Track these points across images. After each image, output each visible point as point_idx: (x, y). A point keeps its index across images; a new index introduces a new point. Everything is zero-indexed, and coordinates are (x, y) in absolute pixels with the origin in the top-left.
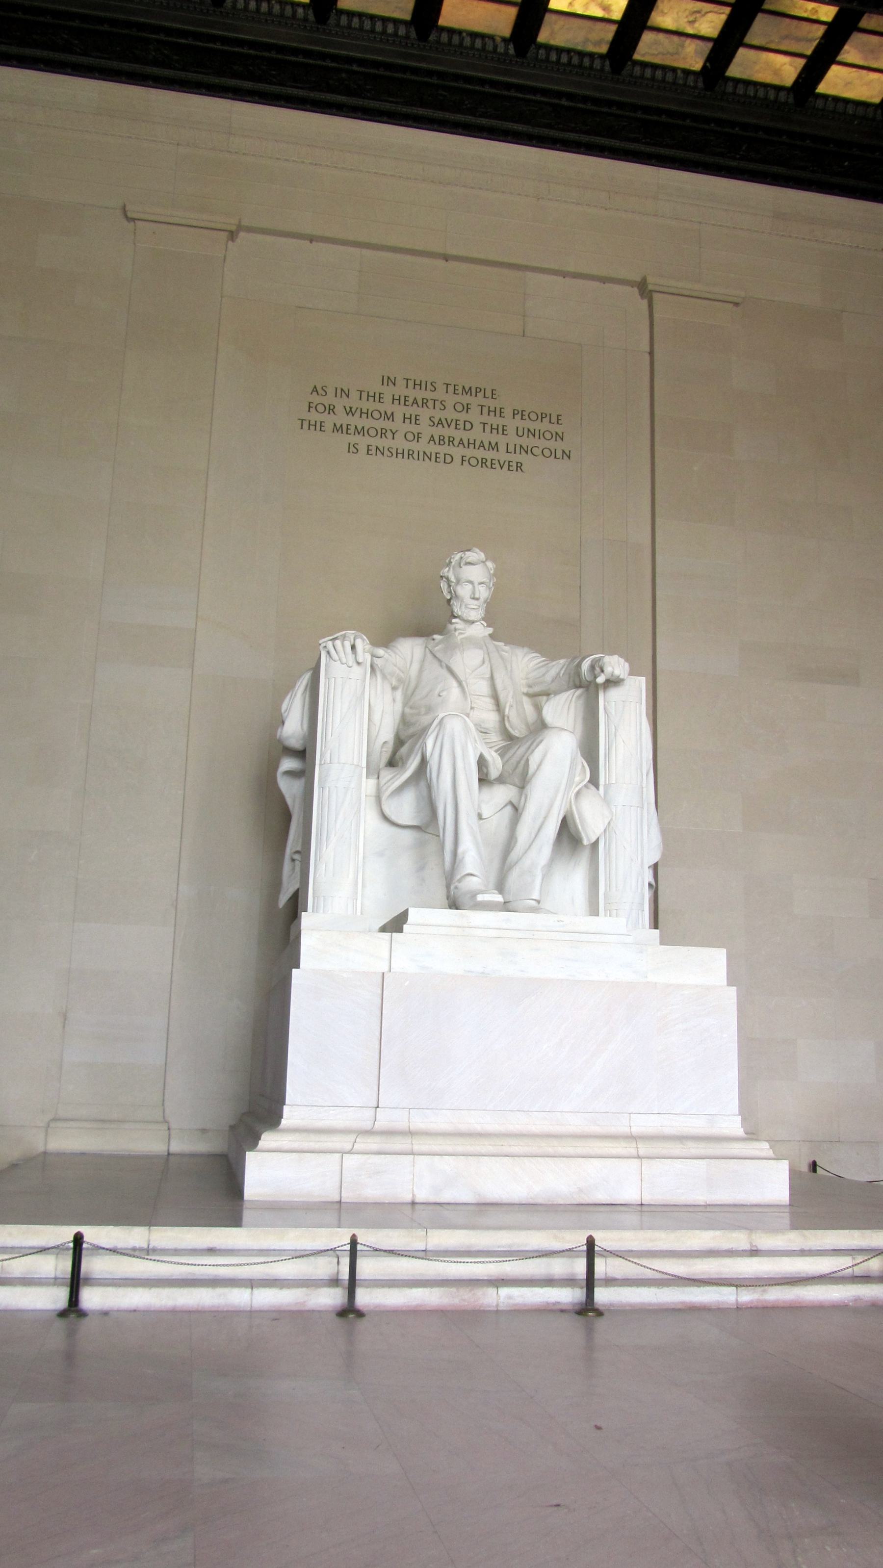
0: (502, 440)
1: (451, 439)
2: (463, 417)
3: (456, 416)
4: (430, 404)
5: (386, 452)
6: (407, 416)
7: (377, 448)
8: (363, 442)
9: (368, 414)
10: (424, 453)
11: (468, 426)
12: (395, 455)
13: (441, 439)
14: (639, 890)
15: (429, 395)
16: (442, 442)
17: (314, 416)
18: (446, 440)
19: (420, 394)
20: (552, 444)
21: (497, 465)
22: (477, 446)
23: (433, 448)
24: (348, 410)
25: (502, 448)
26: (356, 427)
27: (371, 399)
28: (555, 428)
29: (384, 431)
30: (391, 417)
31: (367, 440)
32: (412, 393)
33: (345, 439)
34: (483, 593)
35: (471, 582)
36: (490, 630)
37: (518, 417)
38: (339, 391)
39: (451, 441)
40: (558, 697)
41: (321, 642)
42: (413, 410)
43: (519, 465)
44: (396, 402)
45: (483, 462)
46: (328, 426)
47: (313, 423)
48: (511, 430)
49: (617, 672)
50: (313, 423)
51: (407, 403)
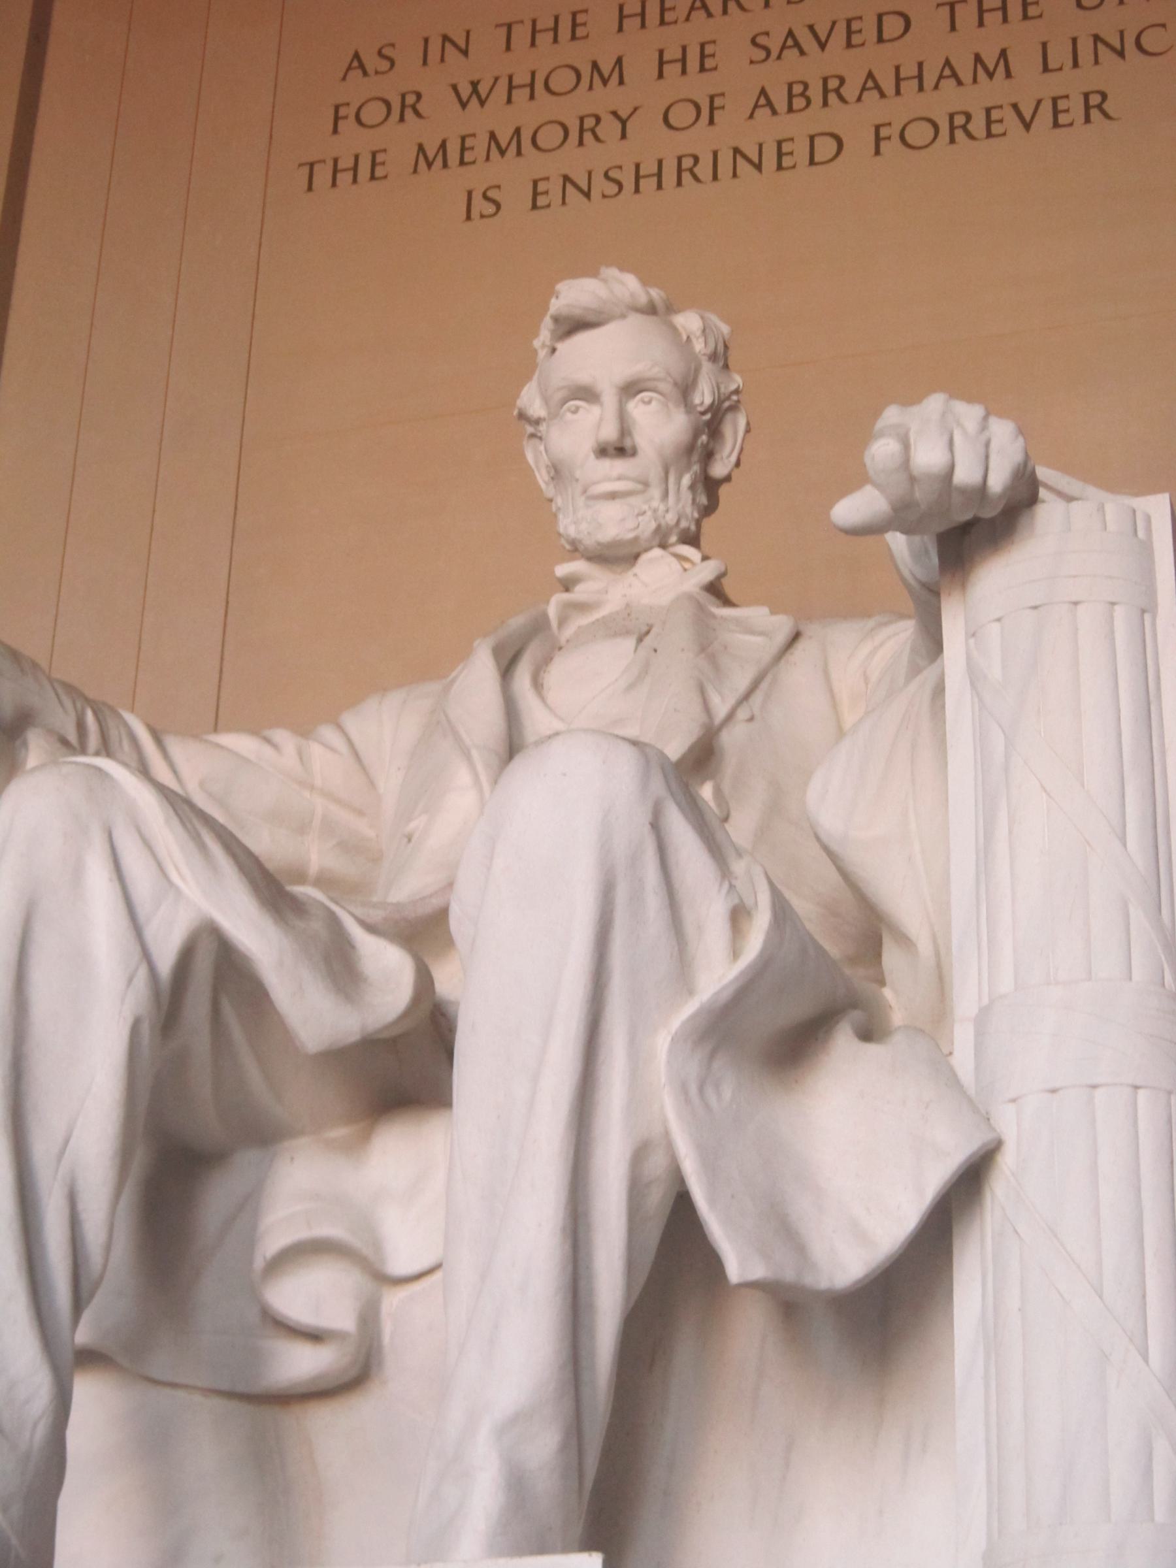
0: (1022, 40)
1: (833, 84)
5: (600, 185)
6: (672, 53)
7: (566, 178)
8: (512, 175)
10: (736, 151)
11: (893, 26)
12: (629, 185)
14: (1160, 1515)
16: (799, 103)
17: (354, 142)
18: (815, 92)
23: (767, 128)
25: (1025, 62)
26: (493, 136)
27: (545, 39)
29: (589, 123)
31: (534, 164)
33: (451, 184)
34: (659, 426)
35: (587, 394)
43: (1095, 100)
45: (958, 126)
47: (346, 162)
49: (928, 456)
50: (346, 162)
51: (669, 16)
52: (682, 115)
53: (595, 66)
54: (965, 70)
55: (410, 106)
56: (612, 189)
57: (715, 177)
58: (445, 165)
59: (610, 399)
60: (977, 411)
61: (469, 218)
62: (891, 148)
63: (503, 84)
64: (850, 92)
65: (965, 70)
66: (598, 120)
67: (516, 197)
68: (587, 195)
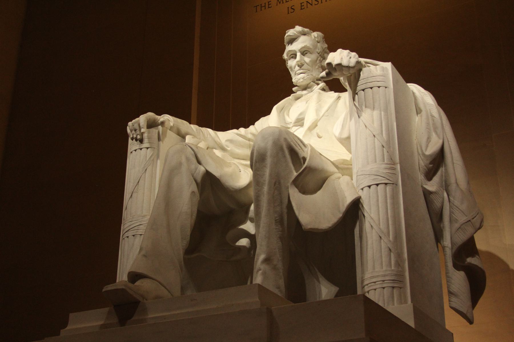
14: (393, 268)
47: (263, 5)
58: (283, 3)
59: (298, 54)
60: (348, 51)
68: (312, 5)
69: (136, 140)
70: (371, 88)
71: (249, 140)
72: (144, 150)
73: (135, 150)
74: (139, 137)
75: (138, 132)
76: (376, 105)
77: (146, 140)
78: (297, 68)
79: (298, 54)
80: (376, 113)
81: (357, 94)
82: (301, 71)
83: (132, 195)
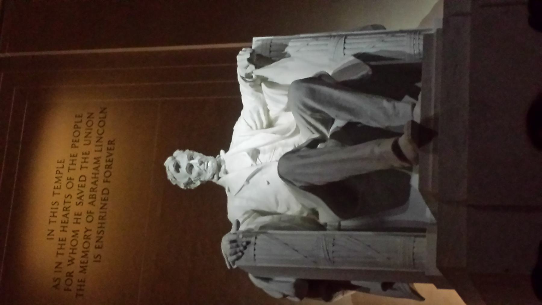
2: (76, 182)
3: (76, 187)
4: (67, 205)
5: (101, 235)
7: (97, 241)
9: (74, 248)
11: (83, 178)
13: (91, 197)
15: (61, 208)
16: (94, 196)
19: (60, 213)
20: (96, 120)
21: (111, 158)
22: (96, 172)
24: (70, 263)
25: (98, 154)
26: (83, 257)
27: (63, 247)
28: (85, 120)
30: (76, 233)
31: (92, 249)
32: (60, 217)
36: (222, 152)
37: (77, 144)
38: (57, 269)
39: (92, 190)
40: (268, 101)
41: (229, 267)
42: (71, 216)
44: (66, 229)
46: (81, 276)
48: (86, 149)
50: (79, 288)
51: (66, 221)
52: (90, 219)
53: (73, 236)
54: (97, 165)
55: (70, 275)
56: (102, 233)
57: (106, 212)
58: (86, 266)
59: (192, 162)
61: (99, 261)
62: (109, 179)
63: (71, 255)
64: (94, 187)
65: (97, 165)
66: (85, 235)
67: (98, 251)
69: (245, 248)
70: (271, 46)
71: (249, 217)
72: (257, 242)
73: (255, 250)
74: (244, 244)
75: (239, 244)
76: (284, 43)
77: (248, 239)
78: (202, 167)
79: (192, 162)
80: (290, 44)
81: (271, 58)
82: (206, 163)
83: (296, 251)
